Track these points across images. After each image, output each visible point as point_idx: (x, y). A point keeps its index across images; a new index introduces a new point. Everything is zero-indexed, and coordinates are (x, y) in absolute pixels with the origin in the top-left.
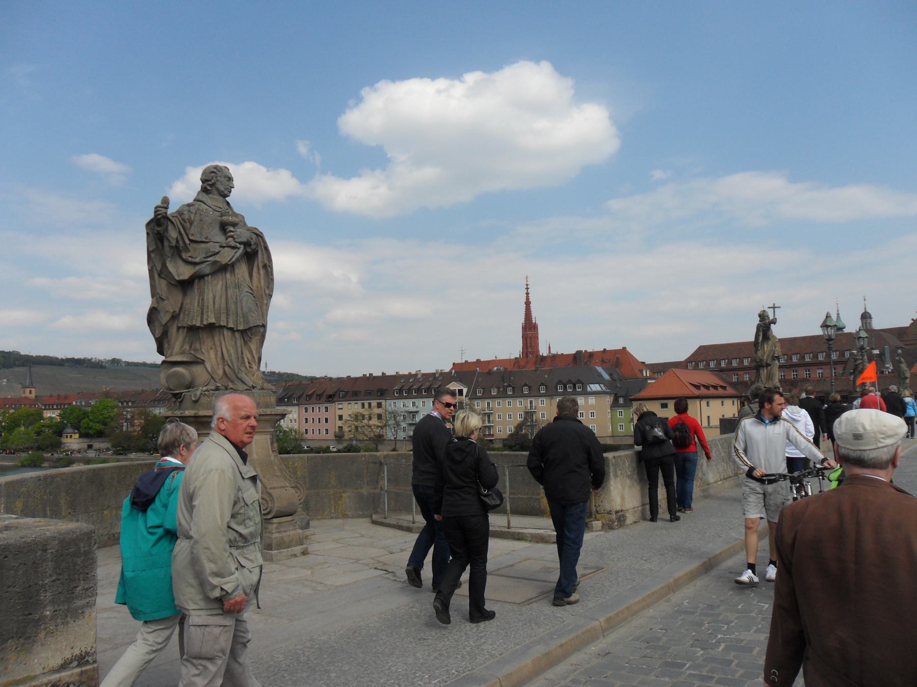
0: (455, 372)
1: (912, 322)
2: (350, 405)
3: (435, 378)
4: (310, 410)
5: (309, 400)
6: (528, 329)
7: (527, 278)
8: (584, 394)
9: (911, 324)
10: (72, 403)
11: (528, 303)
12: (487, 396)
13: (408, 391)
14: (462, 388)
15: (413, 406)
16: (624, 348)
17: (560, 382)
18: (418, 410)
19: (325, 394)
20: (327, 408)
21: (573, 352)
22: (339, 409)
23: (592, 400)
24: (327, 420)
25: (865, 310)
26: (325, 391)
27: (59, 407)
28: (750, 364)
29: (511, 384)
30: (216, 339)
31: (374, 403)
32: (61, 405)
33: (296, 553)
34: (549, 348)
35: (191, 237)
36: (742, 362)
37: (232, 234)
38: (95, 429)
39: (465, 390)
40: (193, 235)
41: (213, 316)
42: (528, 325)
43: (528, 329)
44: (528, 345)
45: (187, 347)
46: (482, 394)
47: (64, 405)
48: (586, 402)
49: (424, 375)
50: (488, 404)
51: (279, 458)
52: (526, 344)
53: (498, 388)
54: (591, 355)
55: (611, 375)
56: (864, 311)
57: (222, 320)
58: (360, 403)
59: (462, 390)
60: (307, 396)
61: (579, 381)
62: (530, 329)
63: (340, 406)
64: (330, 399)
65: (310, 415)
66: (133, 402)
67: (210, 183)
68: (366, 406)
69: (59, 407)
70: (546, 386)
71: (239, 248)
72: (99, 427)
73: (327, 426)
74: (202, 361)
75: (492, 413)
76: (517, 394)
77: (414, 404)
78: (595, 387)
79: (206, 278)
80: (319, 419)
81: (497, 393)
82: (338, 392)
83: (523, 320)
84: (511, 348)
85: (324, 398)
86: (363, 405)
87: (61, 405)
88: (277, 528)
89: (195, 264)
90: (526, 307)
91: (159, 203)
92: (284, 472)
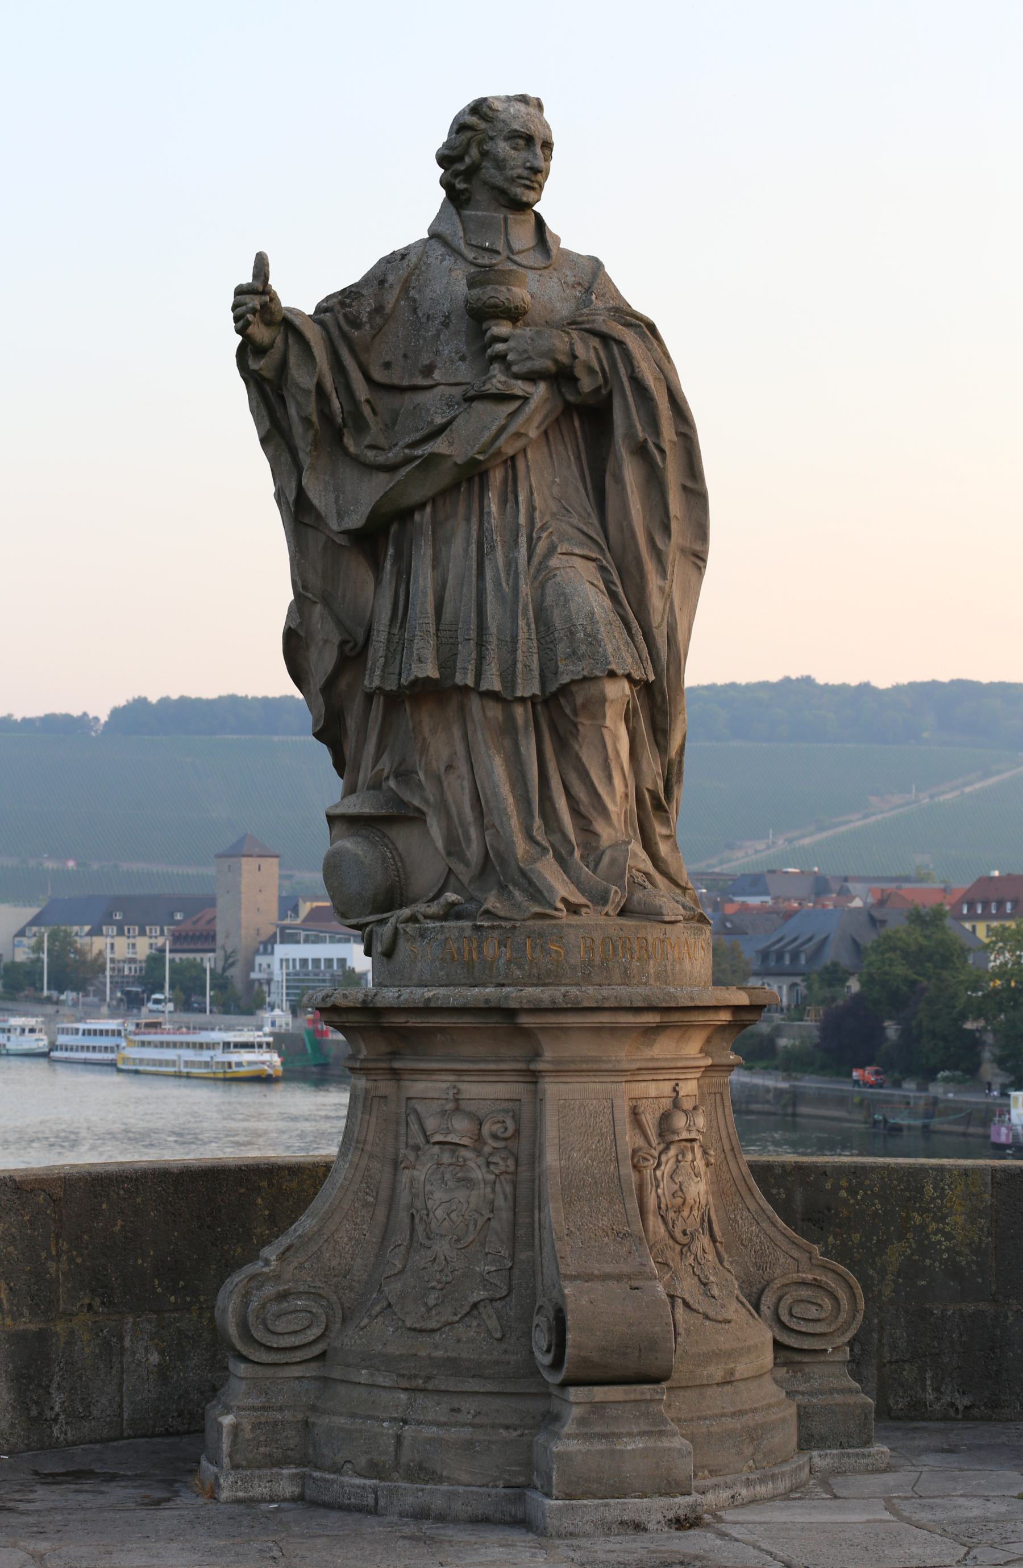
33: (644, 1518)
35: (378, 375)
37: (500, 347)
40: (387, 365)
41: (429, 654)
51: (745, 1170)
57: (459, 665)
67: (460, 167)
71: (525, 399)
74: (416, 815)
79: (417, 517)
88: (582, 1421)
91: (246, 277)
92: (764, 1225)
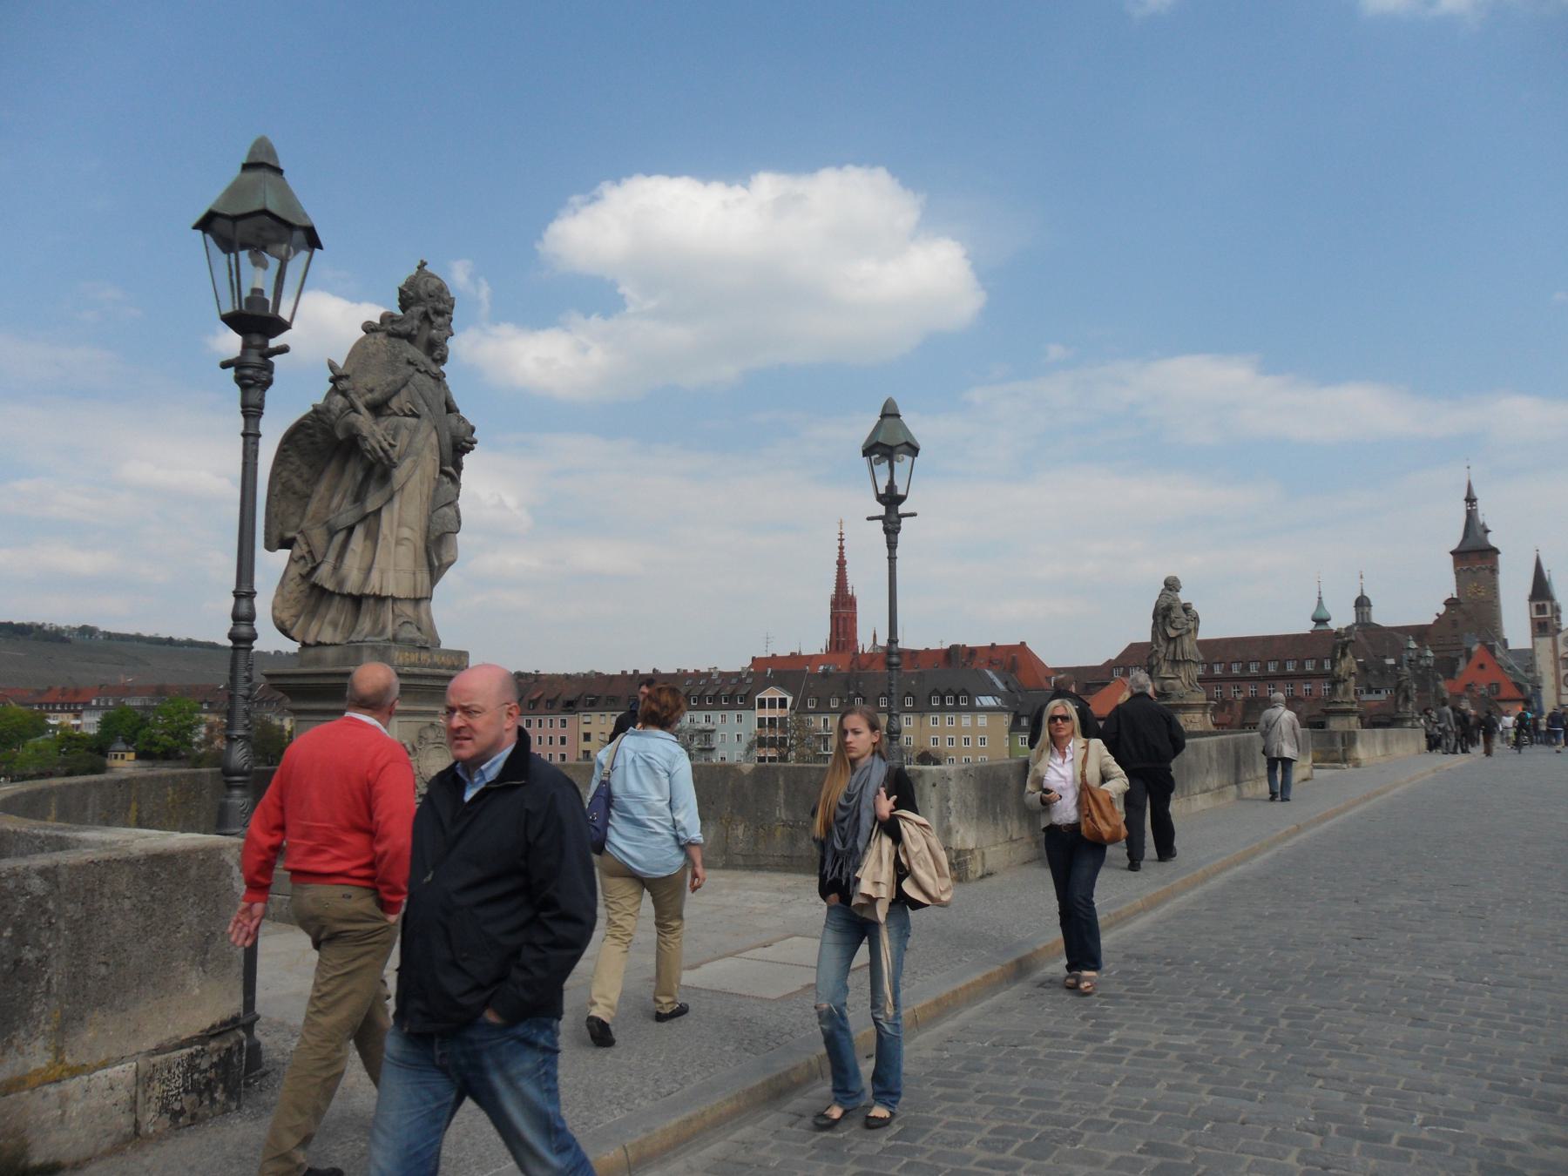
0: (772, 671)
1: (1437, 618)
2: (603, 718)
3: (741, 681)
4: (535, 723)
5: (534, 708)
6: (840, 604)
7: (841, 522)
8: (956, 711)
9: (1436, 621)
10: (91, 702)
11: (841, 563)
13: (699, 698)
14: (785, 696)
15: (706, 721)
16: (1023, 644)
17: (935, 692)
18: (714, 728)
19: (560, 700)
20: (564, 721)
21: (946, 646)
22: (585, 723)
23: (982, 720)
24: (563, 741)
25: (1362, 593)
26: (560, 694)
27: (72, 708)
28: (1223, 672)
29: (860, 692)
30: (1186, 666)
32: (69, 705)
34: (875, 636)
36: (1212, 669)
38: (164, 746)
39: (790, 700)
42: (840, 598)
43: (840, 604)
44: (841, 630)
45: (1171, 670)
46: (817, 706)
47: (76, 704)
48: (974, 722)
49: (721, 674)
50: (826, 721)
52: (838, 628)
53: (841, 698)
54: (973, 652)
55: (1006, 683)
56: (1360, 595)
59: (785, 699)
60: (531, 701)
61: (964, 692)
62: (844, 605)
63: (587, 719)
64: (571, 708)
66: (210, 704)
69: (72, 708)
70: (914, 697)
72: (168, 740)
73: (564, 749)
75: (830, 735)
77: (708, 719)
78: (988, 701)
80: (551, 738)
81: (840, 705)
82: (583, 697)
83: (832, 590)
84: (813, 638)
85: (558, 706)
87: (47, 704)
89: (1177, 629)
90: (839, 569)
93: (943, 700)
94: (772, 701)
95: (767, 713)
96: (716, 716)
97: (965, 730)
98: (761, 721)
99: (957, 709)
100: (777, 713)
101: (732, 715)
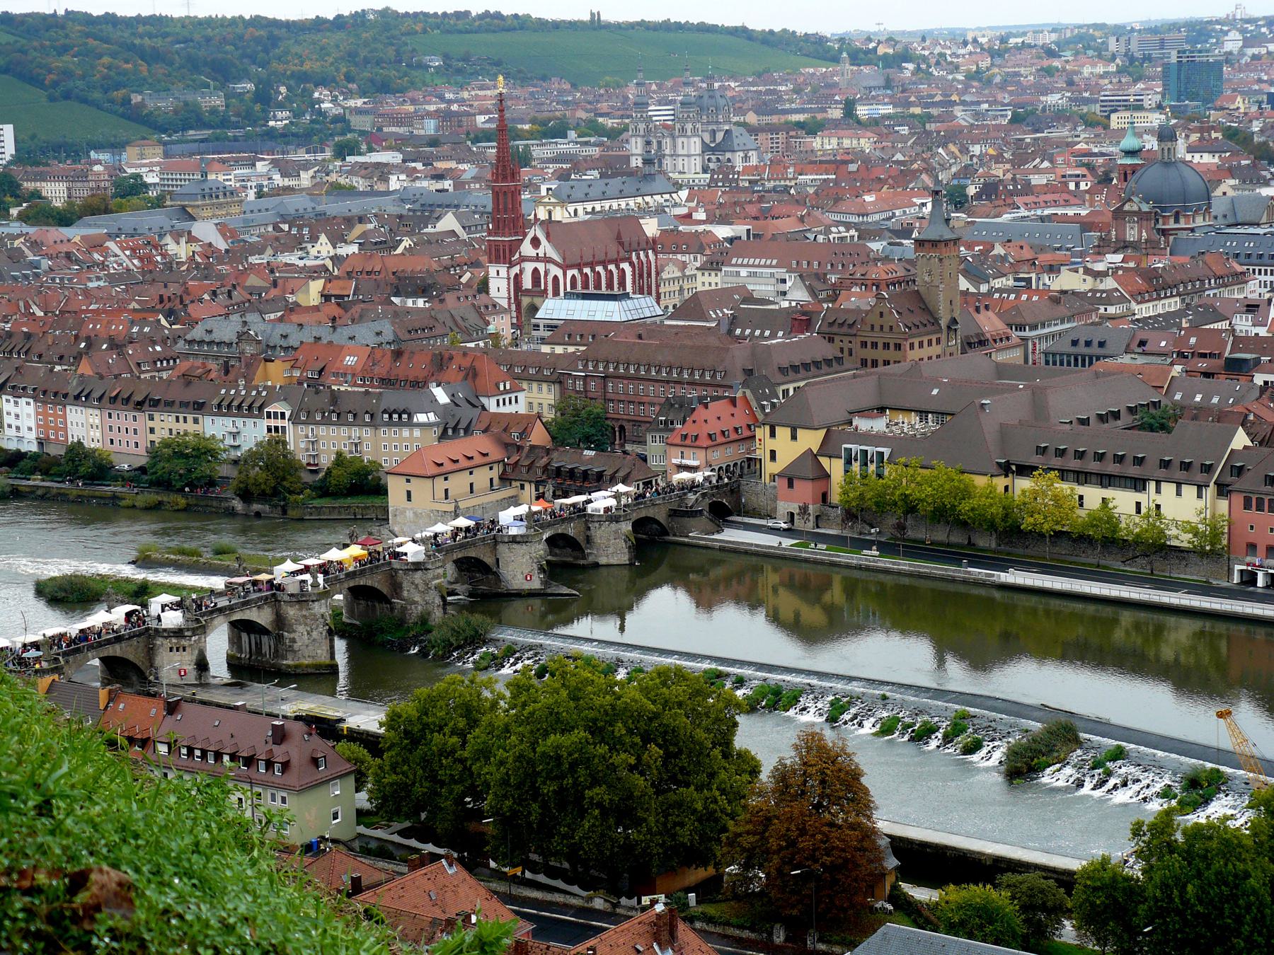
4: (114, 415)
12: (310, 421)
17: (385, 412)
23: (417, 433)
31: (190, 417)
48: (411, 434)
58: (174, 415)
65: (114, 421)
68: (181, 419)
76: (341, 421)
85: (131, 405)
86: (177, 418)
93: (391, 417)
94: (275, 413)
95: (273, 423)
96: (239, 422)
97: (406, 439)
98: (269, 430)
99: (400, 424)
100: (279, 423)
101: (250, 422)
